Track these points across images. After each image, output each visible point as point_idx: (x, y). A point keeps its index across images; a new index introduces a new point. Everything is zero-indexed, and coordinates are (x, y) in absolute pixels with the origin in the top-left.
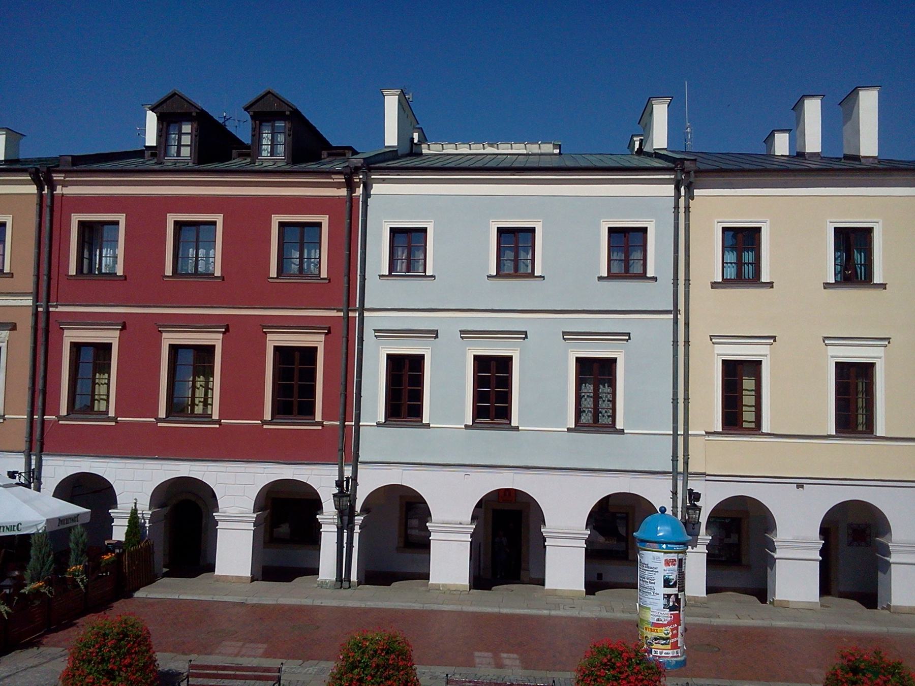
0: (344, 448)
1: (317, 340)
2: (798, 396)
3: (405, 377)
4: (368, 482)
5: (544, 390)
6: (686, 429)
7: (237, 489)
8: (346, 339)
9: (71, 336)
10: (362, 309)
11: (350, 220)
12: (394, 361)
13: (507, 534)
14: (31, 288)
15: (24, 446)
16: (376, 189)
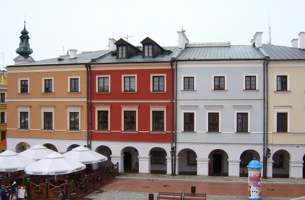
0: (172, 138)
1: (164, 109)
3: (189, 119)
4: (180, 148)
5: (228, 122)
6: (267, 132)
7: (144, 150)
8: (172, 108)
9: (98, 109)
10: (176, 100)
11: (172, 74)
13: (218, 161)
14: (86, 96)
15: (87, 138)
16: (179, 66)
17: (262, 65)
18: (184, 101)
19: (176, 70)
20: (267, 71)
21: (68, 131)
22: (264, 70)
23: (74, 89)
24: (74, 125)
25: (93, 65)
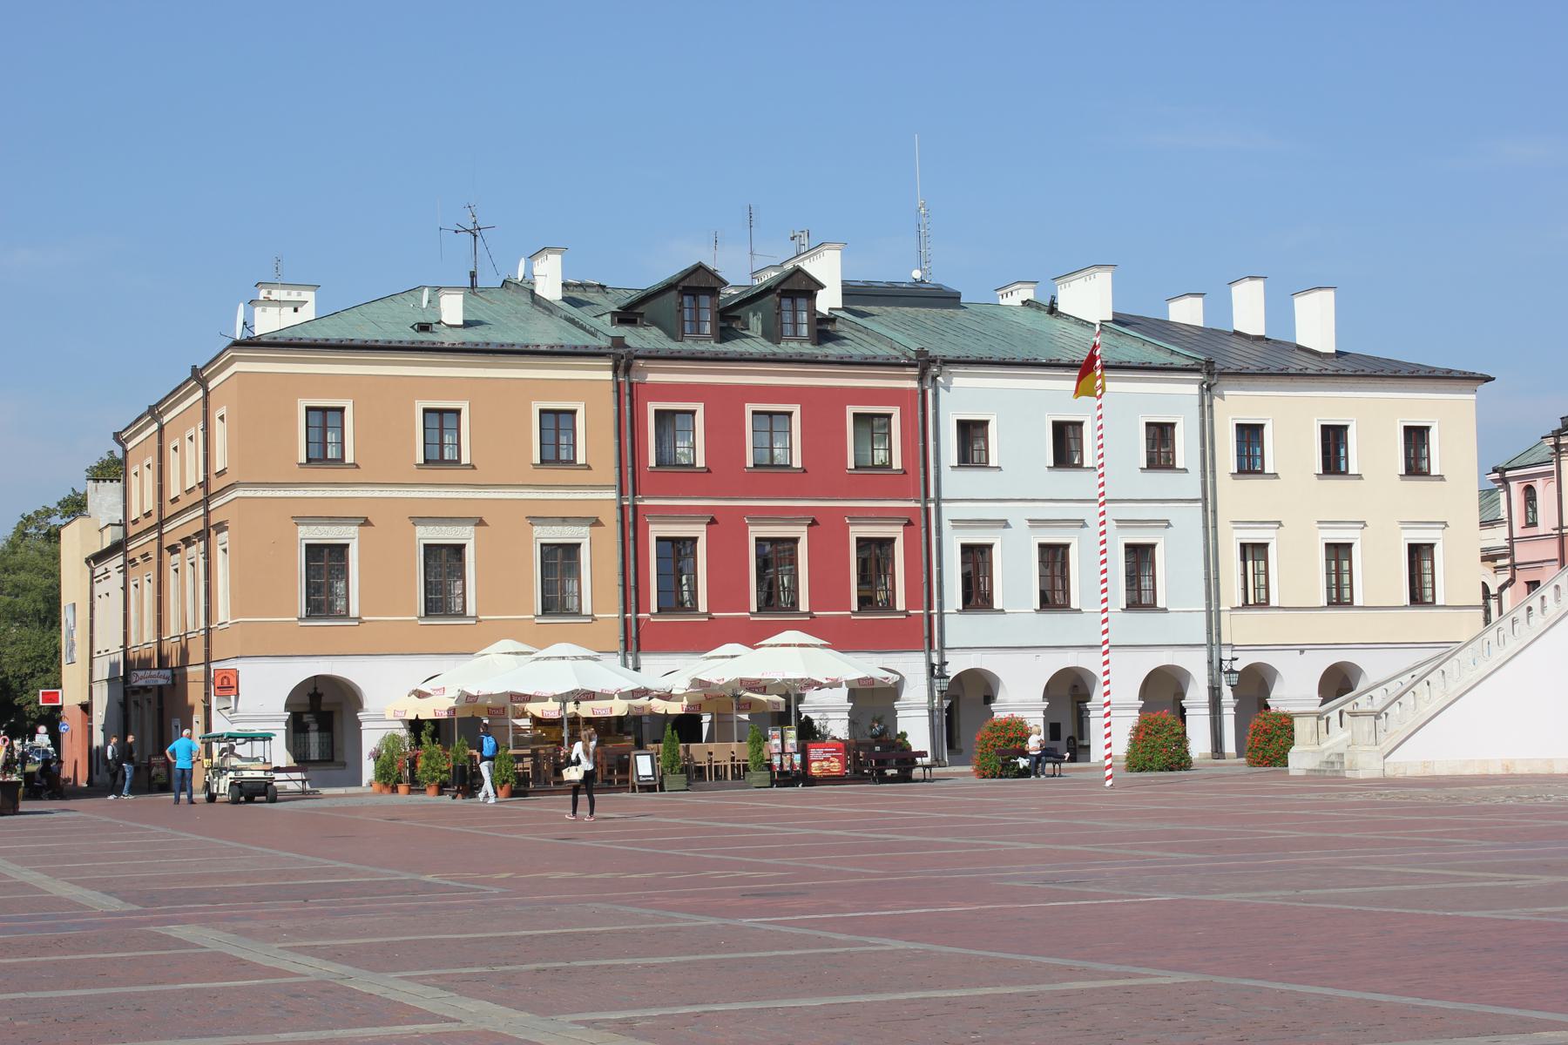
0: (921, 634)
1: (896, 532)
2: (1297, 573)
5: (1095, 574)
6: (1218, 605)
8: (921, 526)
9: (656, 530)
10: (938, 500)
12: (967, 549)
14: (613, 478)
17: (1194, 389)
23: (556, 454)
25: (641, 363)
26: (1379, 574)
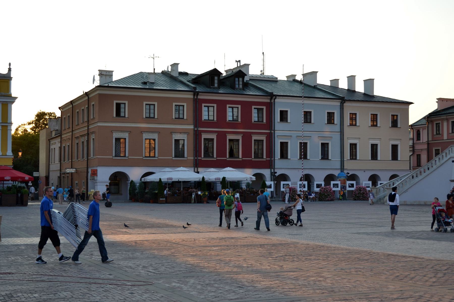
0: (270, 165)
2: (364, 152)
8: (270, 138)
9: (204, 136)
10: (274, 130)
11: (270, 107)
18: (281, 131)
19: (274, 104)
20: (343, 108)
21: (173, 159)
22: (341, 108)
24: (179, 153)
26: (384, 153)
